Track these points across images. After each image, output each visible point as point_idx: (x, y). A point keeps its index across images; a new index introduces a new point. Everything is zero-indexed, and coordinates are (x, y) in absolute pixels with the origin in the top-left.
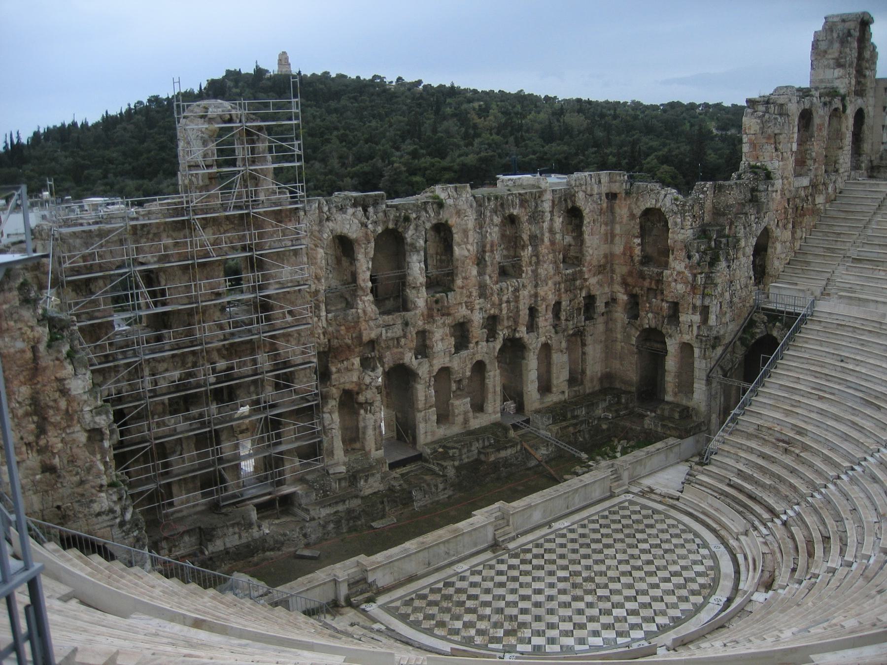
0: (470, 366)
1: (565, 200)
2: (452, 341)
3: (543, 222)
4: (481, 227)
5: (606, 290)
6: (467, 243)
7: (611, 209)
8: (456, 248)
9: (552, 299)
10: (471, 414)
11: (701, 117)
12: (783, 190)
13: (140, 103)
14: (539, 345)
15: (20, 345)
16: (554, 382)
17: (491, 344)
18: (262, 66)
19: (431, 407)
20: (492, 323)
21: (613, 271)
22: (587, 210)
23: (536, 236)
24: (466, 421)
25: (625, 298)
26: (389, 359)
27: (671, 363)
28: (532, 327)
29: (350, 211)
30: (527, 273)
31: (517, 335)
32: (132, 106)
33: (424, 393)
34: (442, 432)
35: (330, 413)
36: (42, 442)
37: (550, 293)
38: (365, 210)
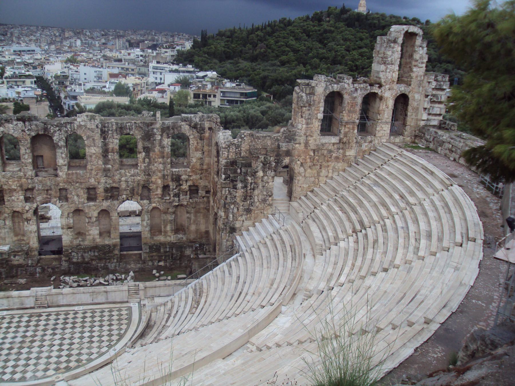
0: (97, 211)
1: (173, 129)
2: (85, 196)
3: (154, 140)
4: (105, 139)
7: (210, 139)
8: (87, 148)
10: (98, 237)
13: (275, 22)
16: (163, 230)
22: (192, 137)
23: (148, 147)
29: (15, 123)
30: (141, 167)
32: (270, 23)
34: (76, 242)
35: (4, 220)
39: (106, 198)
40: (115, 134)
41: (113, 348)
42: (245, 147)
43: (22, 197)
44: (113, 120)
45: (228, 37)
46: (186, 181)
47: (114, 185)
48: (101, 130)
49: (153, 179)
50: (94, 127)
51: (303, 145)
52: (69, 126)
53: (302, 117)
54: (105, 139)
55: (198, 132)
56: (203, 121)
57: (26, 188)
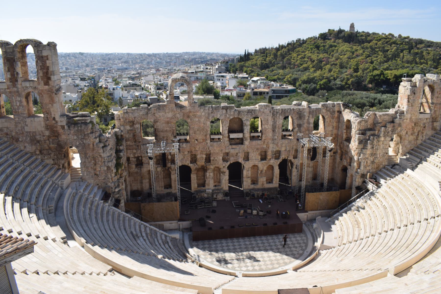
1: (316, 112)
2: (260, 157)
4: (274, 119)
6: (267, 125)
10: (265, 182)
12: (411, 118)
13: (293, 41)
15: (89, 143)
17: (276, 160)
18: (342, 29)
19: (249, 177)
24: (263, 184)
26: (232, 160)
28: (295, 157)
29: (221, 111)
33: (246, 173)
35: (209, 173)
36: (95, 167)
38: (227, 111)
39: (272, 158)
40: (281, 117)
41: (306, 251)
42: (370, 121)
43: (221, 158)
44: (279, 107)
45: (262, 53)
47: (278, 149)
48: (273, 114)
50: (268, 112)
51: (409, 120)
52: (253, 112)
53: (408, 101)
55: (331, 114)
56: (334, 106)
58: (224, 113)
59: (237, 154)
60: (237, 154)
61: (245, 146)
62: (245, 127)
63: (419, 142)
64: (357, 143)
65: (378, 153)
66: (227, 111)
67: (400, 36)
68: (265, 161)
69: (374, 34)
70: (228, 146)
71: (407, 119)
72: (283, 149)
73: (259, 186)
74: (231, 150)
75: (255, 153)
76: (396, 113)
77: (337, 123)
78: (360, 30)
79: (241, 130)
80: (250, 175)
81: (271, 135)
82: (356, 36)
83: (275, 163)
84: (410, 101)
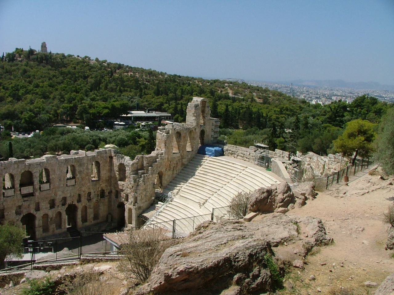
0: (55, 213)
1: (93, 159)
2: (49, 206)
3: (84, 166)
4: (60, 169)
5: (109, 188)
6: (54, 175)
9: (87, 191)
10: (55, 229)
11: (226, 87)
12: (168, 158)
14: (82, 207)
16: (88, 218)
18: (33, 48)
20: (65, 199)
21: (111, 182)
23: (81, 171)
24: (53, 231)
25: (114, 191)
26: (25, 212)
27: (126, 214)
28: (79, 201)
31: (73, 203)
33: (38, 222)
34: (44, 234)
37: (86, 189)
43: (14, 212)
44: (63, 158)
46: (99, 188)
47: (64, 196)
49: (83, 190)
52: (41, 164)
53: (165, 145)
54: (60, 169)
57: (17, 205)
58: (16, 167)
59: (29, 205)
60: (29, 207)
61: (36, 197)
62: (35, 179)
63: (175, 175)
64: (133, 183)
65: (148, 188)
66: (18, 166)
67: (97, 60)
68: (54, 209)
69: (70, 56)
70: (21, 199)
71: (165, 159)
72: (69, 195)
73: (50, 233)
74: (24, 203)
75: (45, 202)
76: (157, 155)
77: (109, 166)
78: (54, 52)
79: (31, 183)
80: (41, 224)
81: (57, 184)
82: (51, 58)
83: (63, 210)
84: (167, 145)
